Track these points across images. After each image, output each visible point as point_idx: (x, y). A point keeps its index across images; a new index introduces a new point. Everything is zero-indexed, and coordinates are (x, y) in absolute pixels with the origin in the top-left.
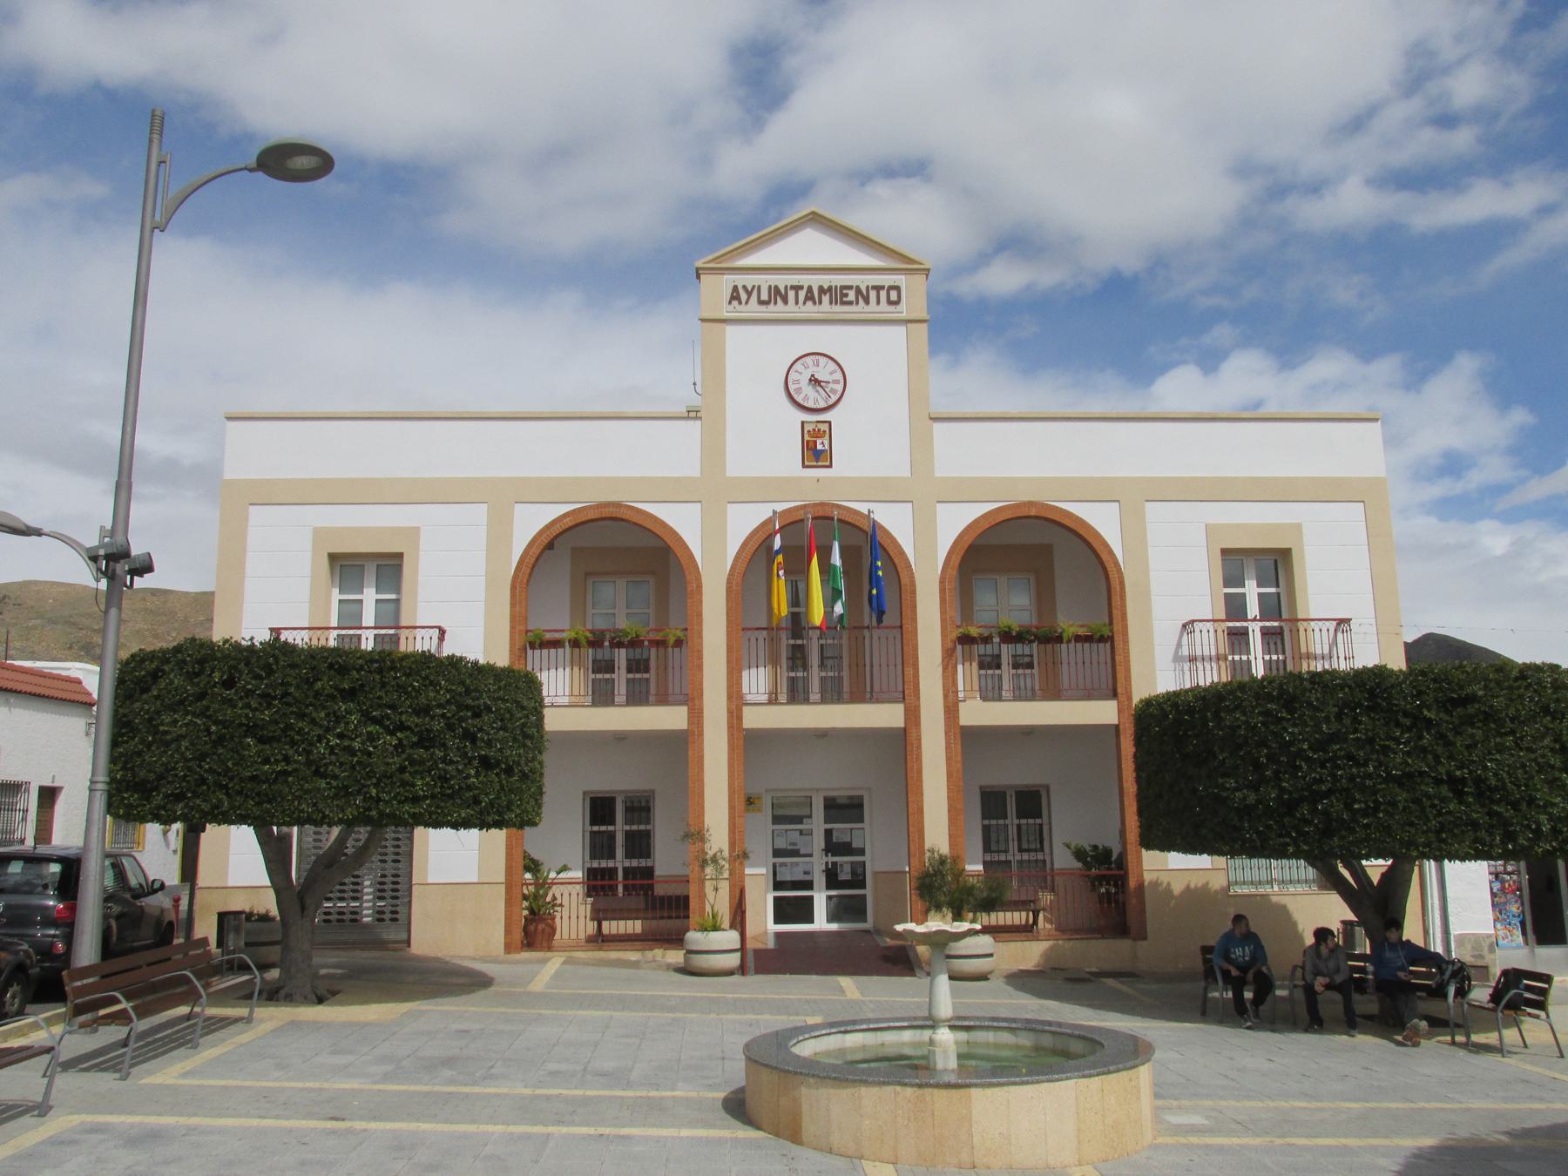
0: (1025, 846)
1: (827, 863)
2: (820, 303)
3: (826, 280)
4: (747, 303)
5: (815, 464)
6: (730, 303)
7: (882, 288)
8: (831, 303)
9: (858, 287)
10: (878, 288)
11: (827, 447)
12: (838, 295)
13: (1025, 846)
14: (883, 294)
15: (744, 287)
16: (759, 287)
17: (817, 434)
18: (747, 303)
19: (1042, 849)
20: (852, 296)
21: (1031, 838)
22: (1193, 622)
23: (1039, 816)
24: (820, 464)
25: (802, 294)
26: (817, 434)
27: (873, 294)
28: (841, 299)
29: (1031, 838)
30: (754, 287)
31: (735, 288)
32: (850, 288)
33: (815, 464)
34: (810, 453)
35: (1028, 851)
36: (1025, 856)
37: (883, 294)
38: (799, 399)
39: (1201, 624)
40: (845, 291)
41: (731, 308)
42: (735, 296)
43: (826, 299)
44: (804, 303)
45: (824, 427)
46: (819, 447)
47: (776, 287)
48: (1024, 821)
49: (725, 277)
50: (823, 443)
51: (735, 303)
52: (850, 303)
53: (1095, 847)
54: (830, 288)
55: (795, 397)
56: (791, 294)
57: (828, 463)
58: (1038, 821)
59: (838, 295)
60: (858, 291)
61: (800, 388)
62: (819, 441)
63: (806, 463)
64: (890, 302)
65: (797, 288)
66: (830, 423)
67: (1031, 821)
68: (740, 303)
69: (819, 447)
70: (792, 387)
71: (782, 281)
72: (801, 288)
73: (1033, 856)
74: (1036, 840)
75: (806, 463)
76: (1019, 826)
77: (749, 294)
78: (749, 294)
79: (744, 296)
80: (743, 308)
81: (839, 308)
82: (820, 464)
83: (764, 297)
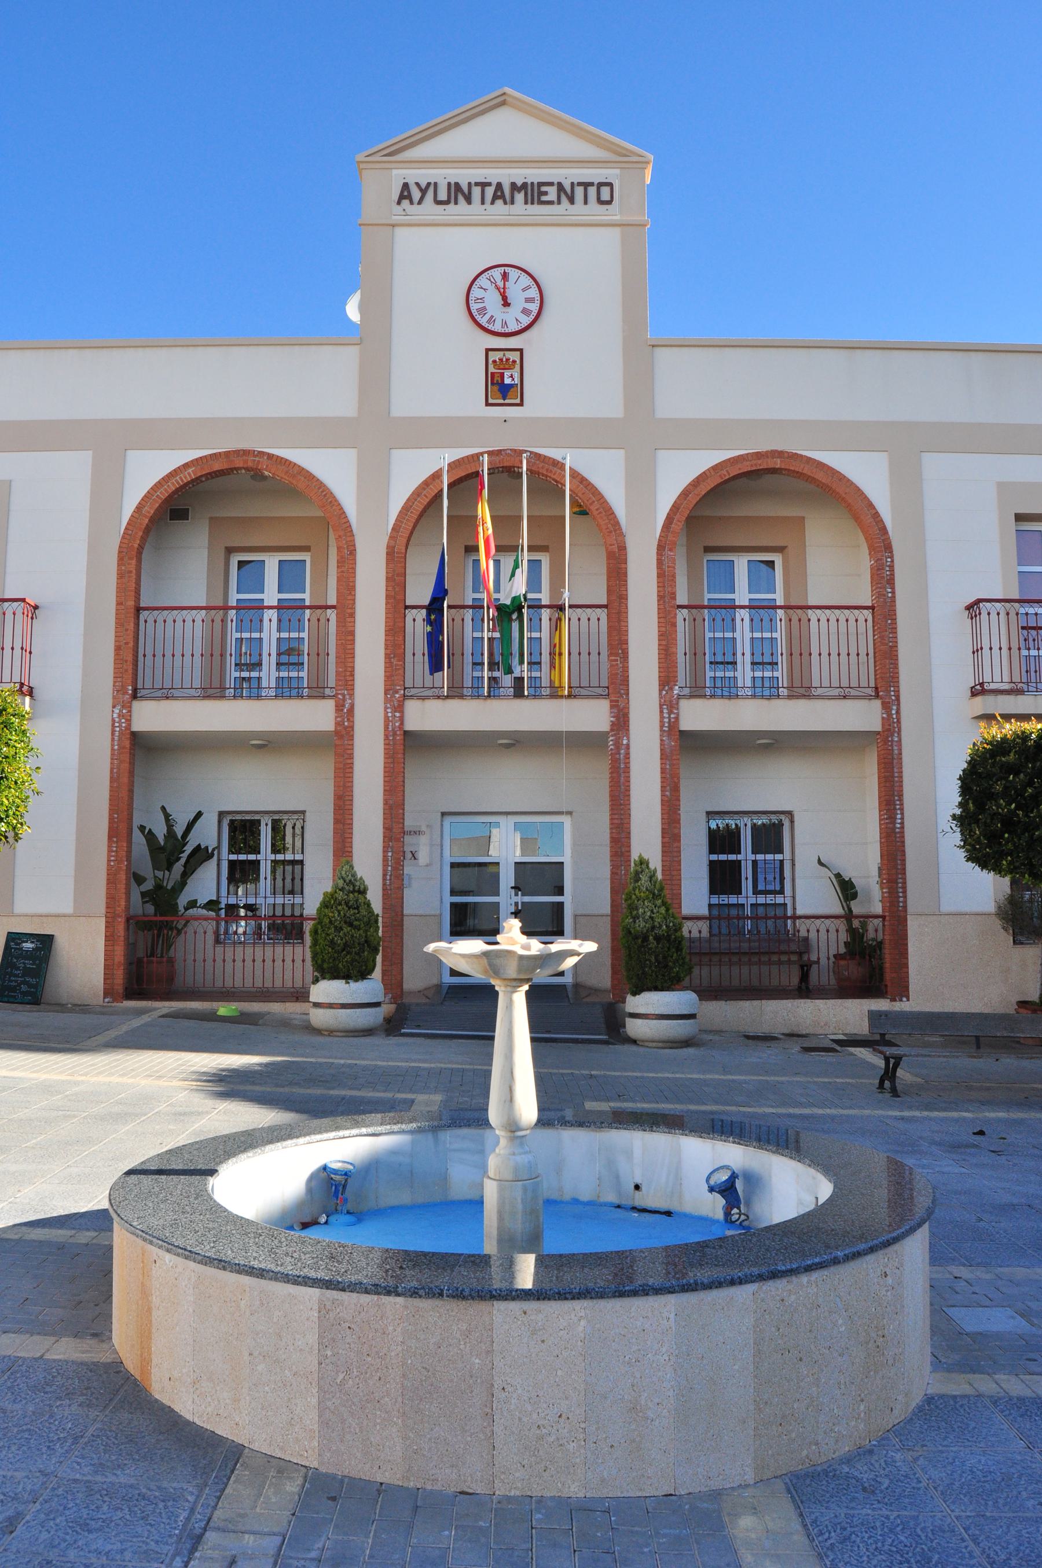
0: (761, 887)
1: (516, 904)
2: (512, 202)
3: (519, 175)
4: (420, 203)
5: (501, 401)
6: (399, 203)
7: (592, 184)
8: (526, 203)
9: (560, 185)
10: (586, 185)
11: (517, 381)
12: (534, 193)
13: (761, 887)
14: (592, 191)
15: (417, 184)
16: (436, 184)
17: (507, 364)
18: (420, 203)
19: (781, 892)
20: (552, 193)
21: (770, 877)
22: (979, 601)
23: (780, 851)
24: (507, 401)
25: (490, 191)
26: (505, 364)
27: (579, 191)
28: (539, 199)
29: (770, 877)
30: (429, 184)
31: (406, 186)
32: (551, 184)
33: (501, 401)
34: (496, 388)
35: (766, 892)
36: (761, 900)
37: (592, 191)
38: (483, 321)
39: (988, 604)
40: (544, 189)
41: (398, 209)
42: (405, 194)
43: (520, 197)
44: (492, 203)
45: (514, 356)
46: (507, 381)
47: (457, 184)
48: (760, 857)
49: (395, 172)
50: (512, 376)
51: (405, 203)
52: (551, 203)
53: (361, 878)
54: (524, 186)
55: (478, 318)
56: (476, 191)
57: (518, 401)
58: (778, 857)
59: (534, 193)
60: (560, 187)
61: (485, 308)
62: (507, 373)
63: (491, 401)
64: (600, 202)
65: (484, 185)
66: (521, 351)
67: (769, 857)
68: (412, 203)
69: (507, 381)
70: (474, 307)
71: (464, 176)
72: (489, 184)
73: (770, 899)
74: (775, 878)
75: (491, 401)
76: (755, 863)
77: (424, 192)
78: (424, 192)
79: (416, 194)
80: (415, 209)
81: (536, 209)
82: (507, 401)
83: (443, 196)
